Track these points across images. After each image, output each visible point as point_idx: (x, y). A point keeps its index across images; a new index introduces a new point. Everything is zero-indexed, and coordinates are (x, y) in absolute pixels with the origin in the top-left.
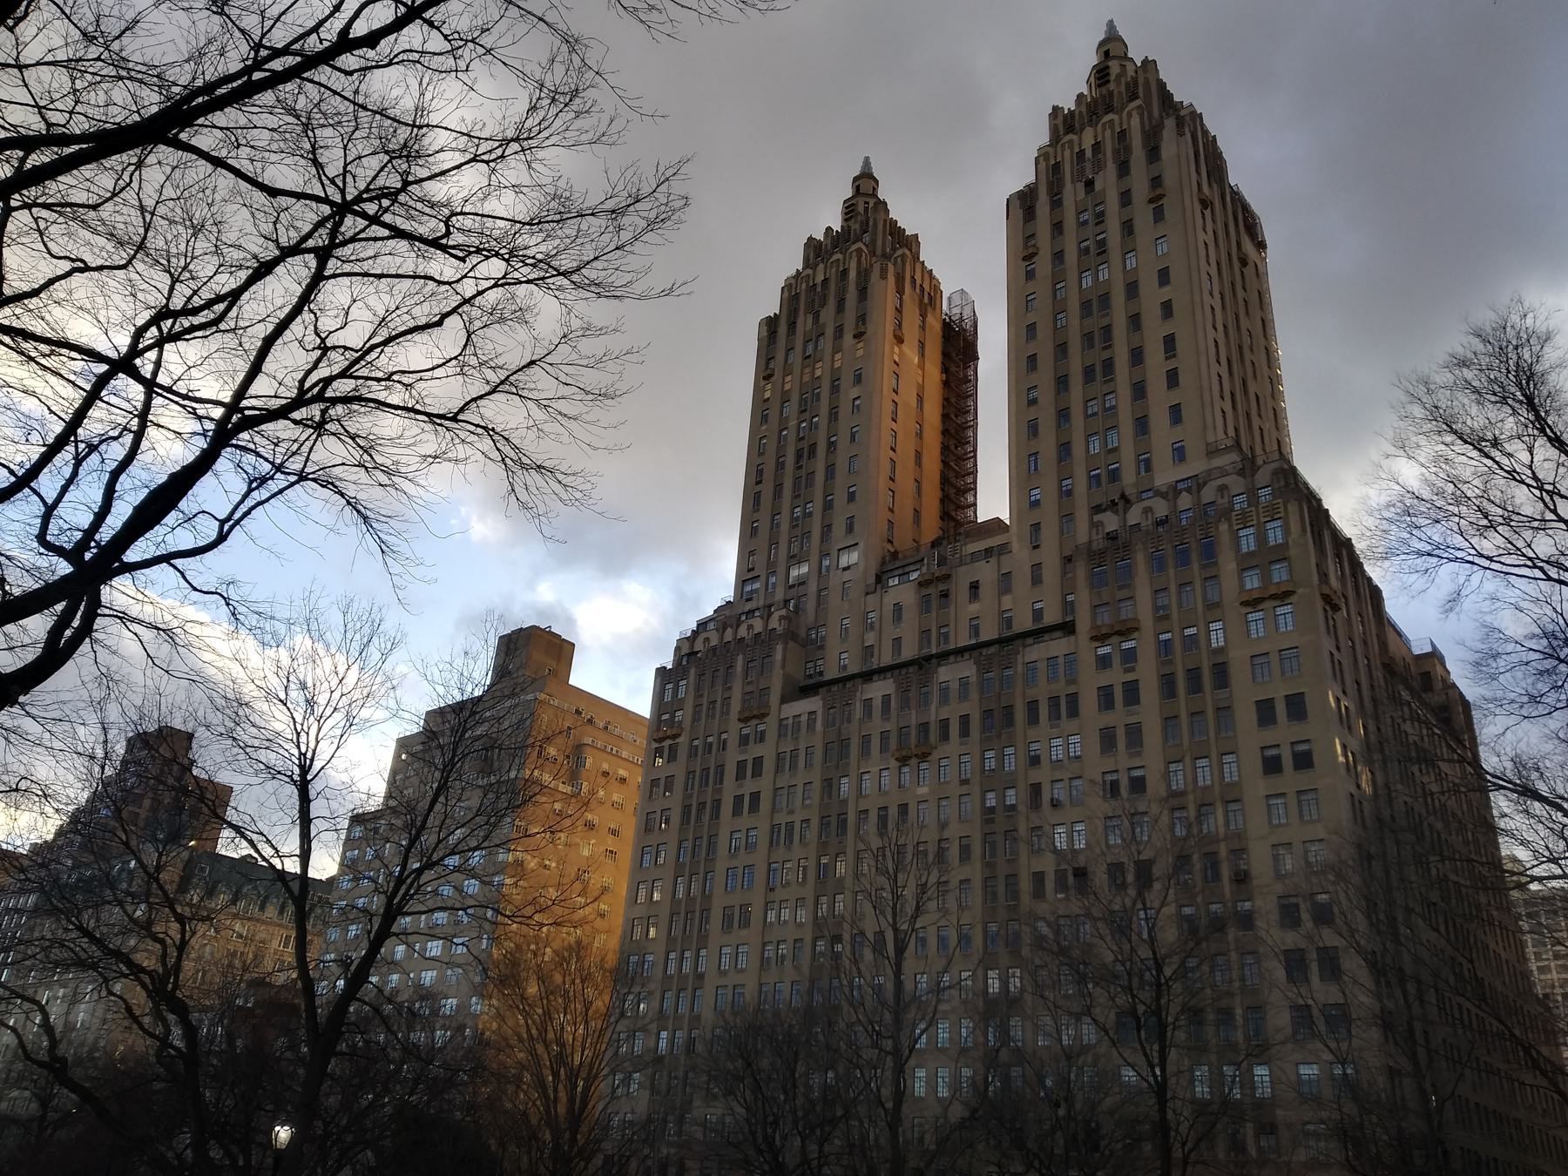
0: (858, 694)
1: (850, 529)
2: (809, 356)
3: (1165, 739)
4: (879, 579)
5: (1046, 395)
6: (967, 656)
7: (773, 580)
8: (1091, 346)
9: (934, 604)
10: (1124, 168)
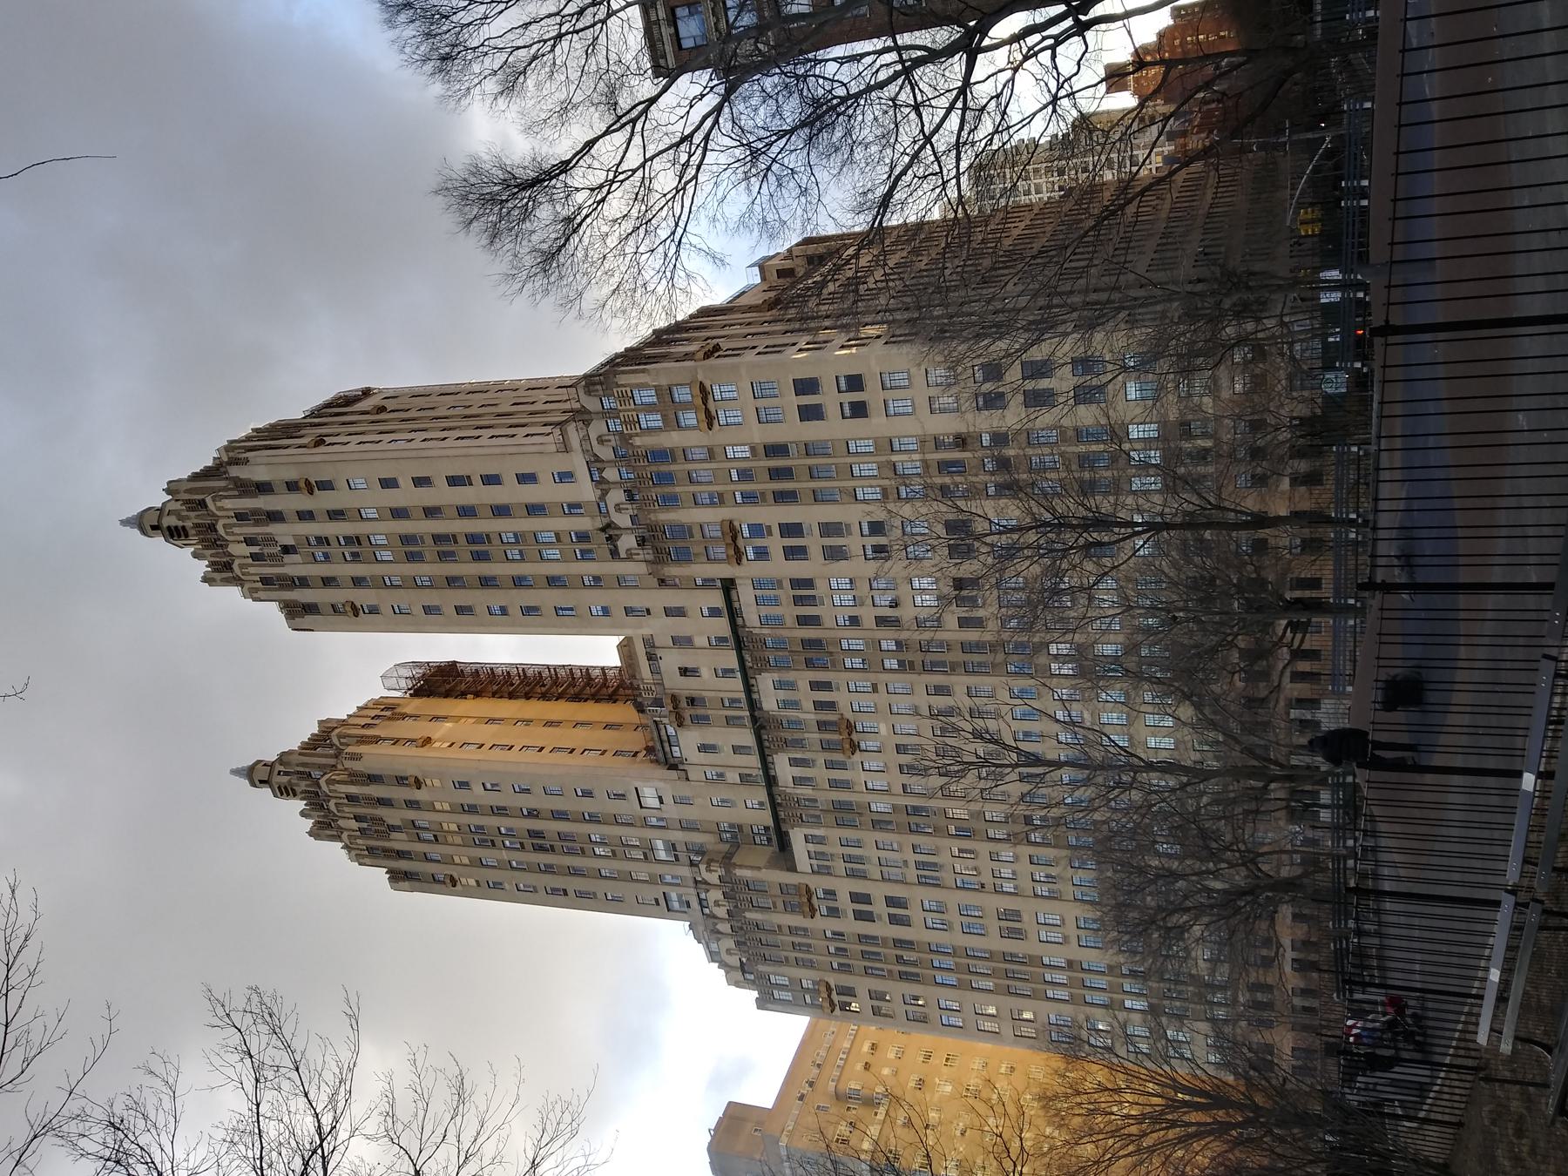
0: (788, 790)
1: (622, 796)
2: (435, 836)
3: (835, 501)
4: (673, 767)
5: (496, 598)
6: (752, 682)
7: (668, 879)
8: (452, 554)
9: (700, 711)
10: (275, 517)
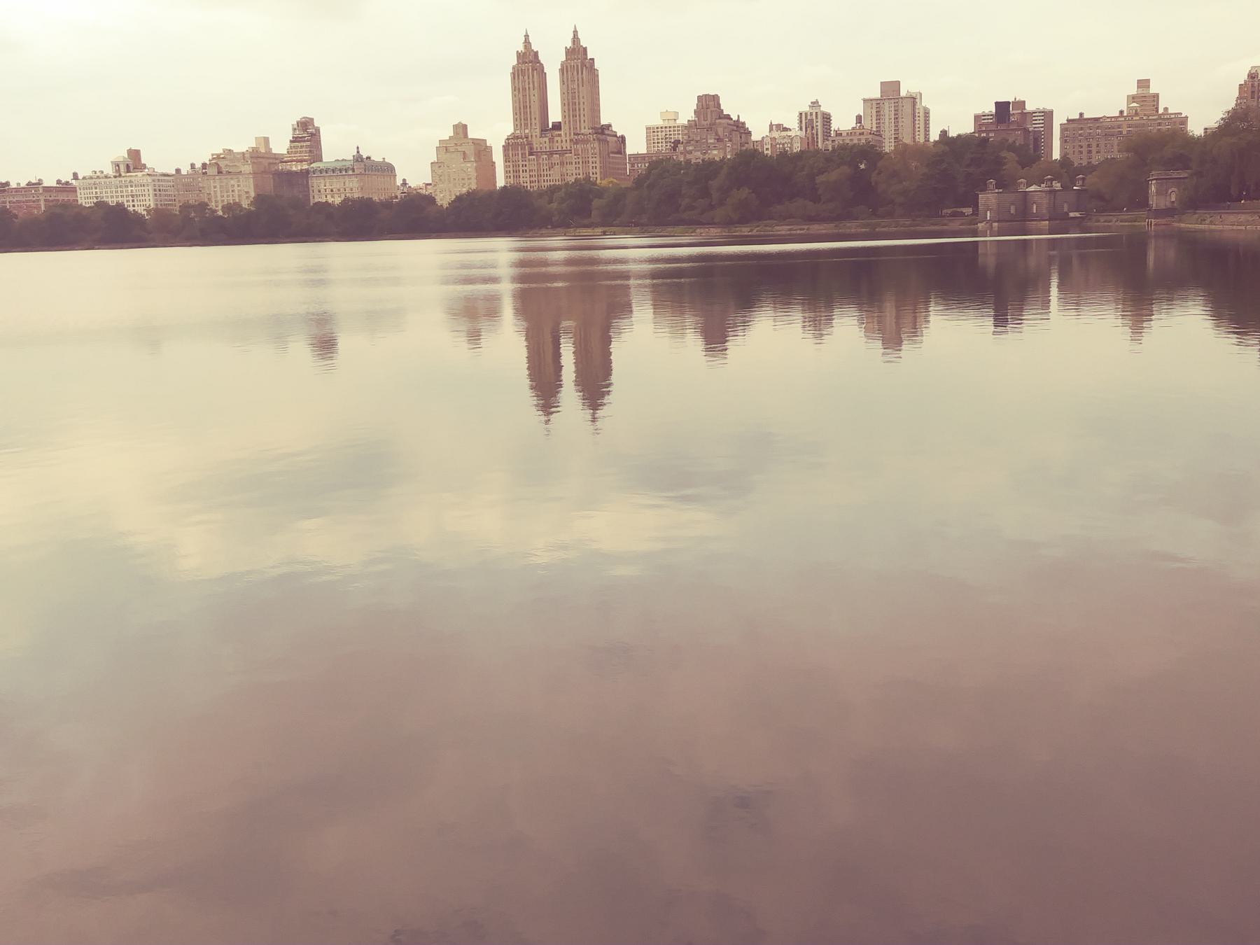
10: (578, 73)
